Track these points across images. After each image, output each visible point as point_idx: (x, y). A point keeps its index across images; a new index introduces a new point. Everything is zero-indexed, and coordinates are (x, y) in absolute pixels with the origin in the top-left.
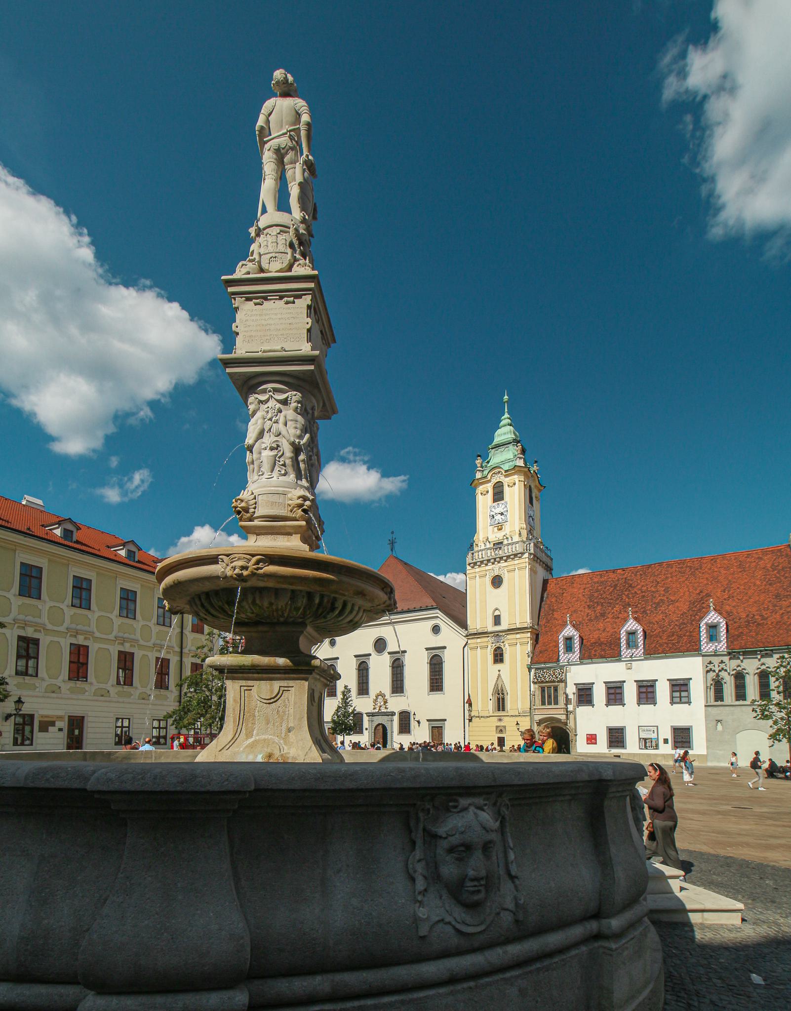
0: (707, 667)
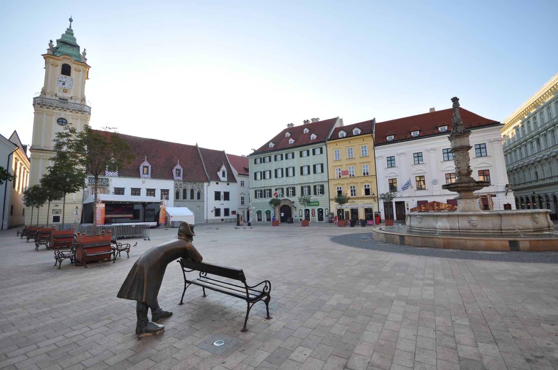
0: (175, 185)
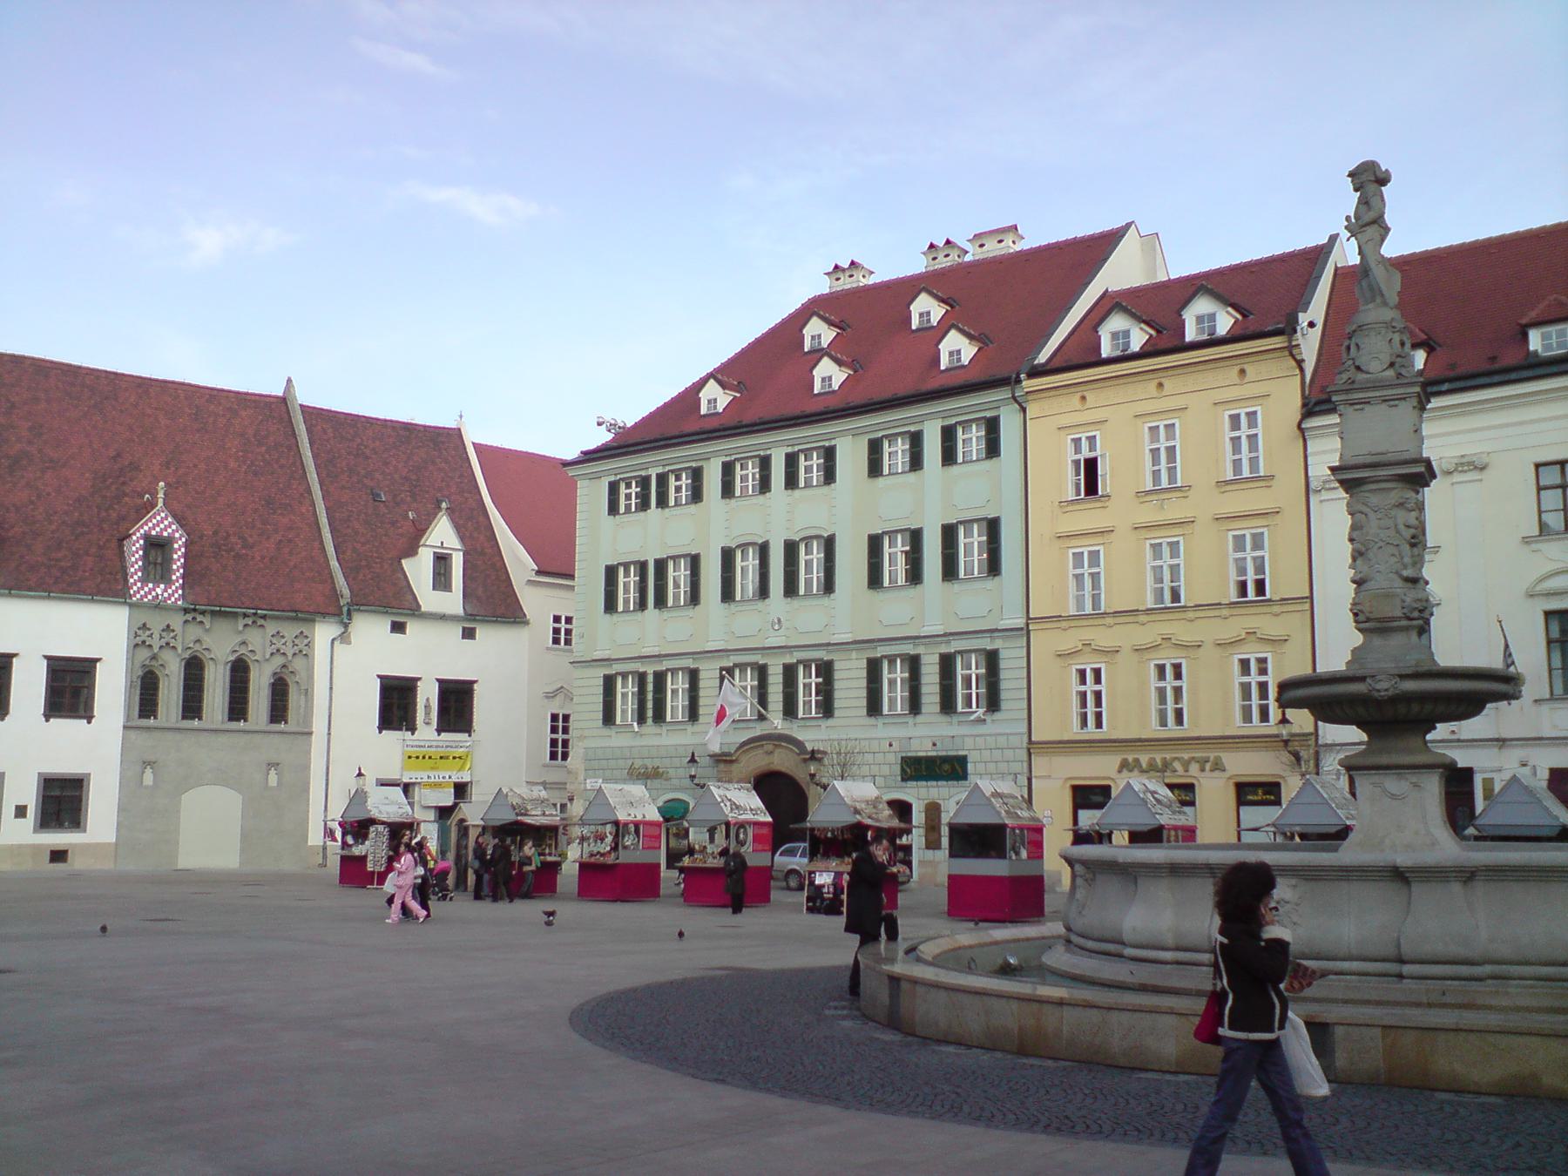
0: (136, 635)
